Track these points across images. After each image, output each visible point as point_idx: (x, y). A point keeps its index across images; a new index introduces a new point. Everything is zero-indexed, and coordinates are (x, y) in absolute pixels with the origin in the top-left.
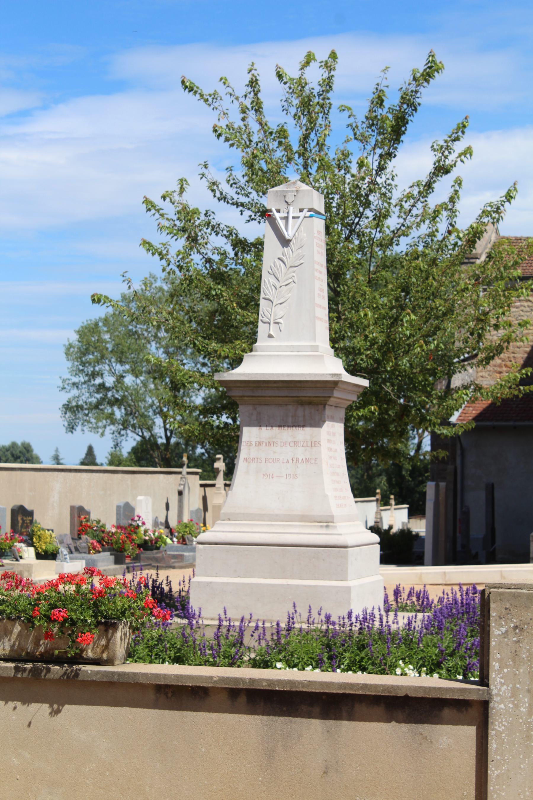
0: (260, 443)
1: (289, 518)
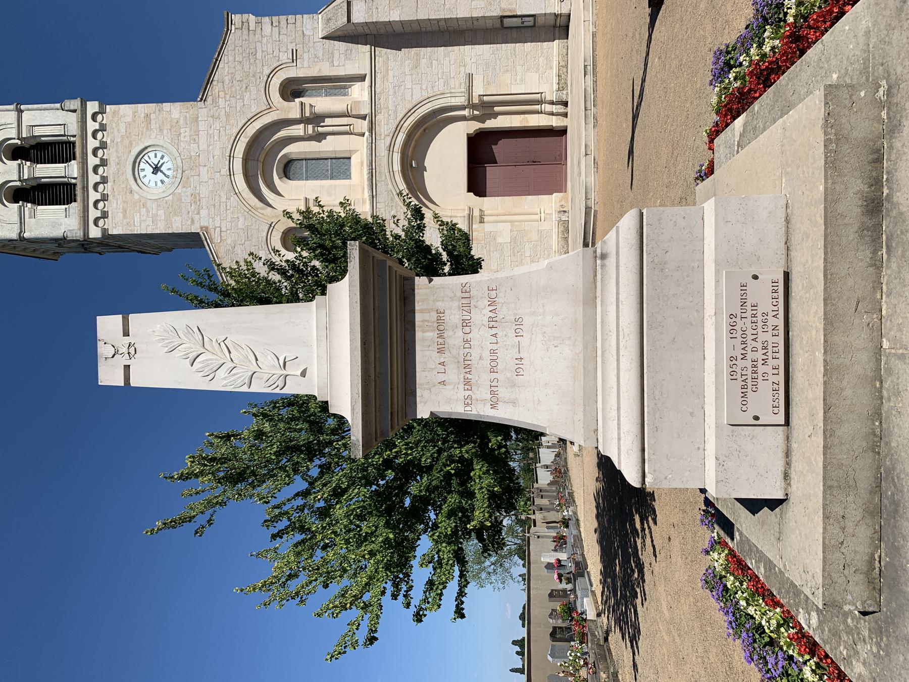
0: (467, 382)
1: (589, 326)
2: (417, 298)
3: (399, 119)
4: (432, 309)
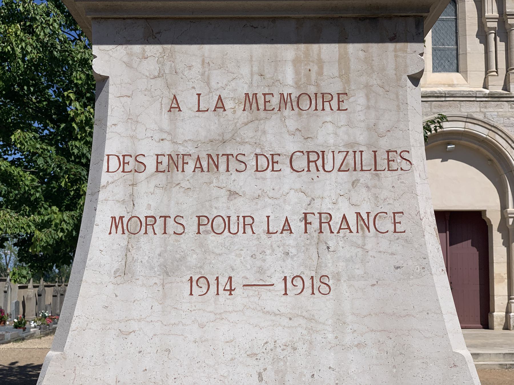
2: (375, 48)
3: (505, 129)
4: (348, 82)
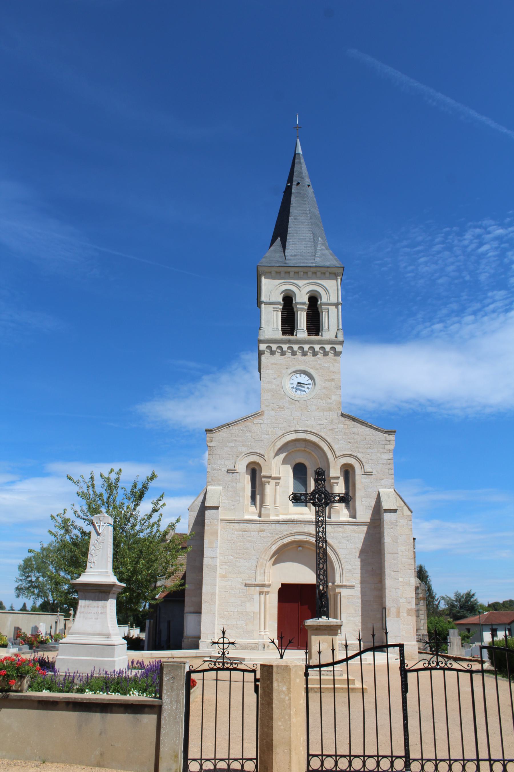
0: (85, 606)
